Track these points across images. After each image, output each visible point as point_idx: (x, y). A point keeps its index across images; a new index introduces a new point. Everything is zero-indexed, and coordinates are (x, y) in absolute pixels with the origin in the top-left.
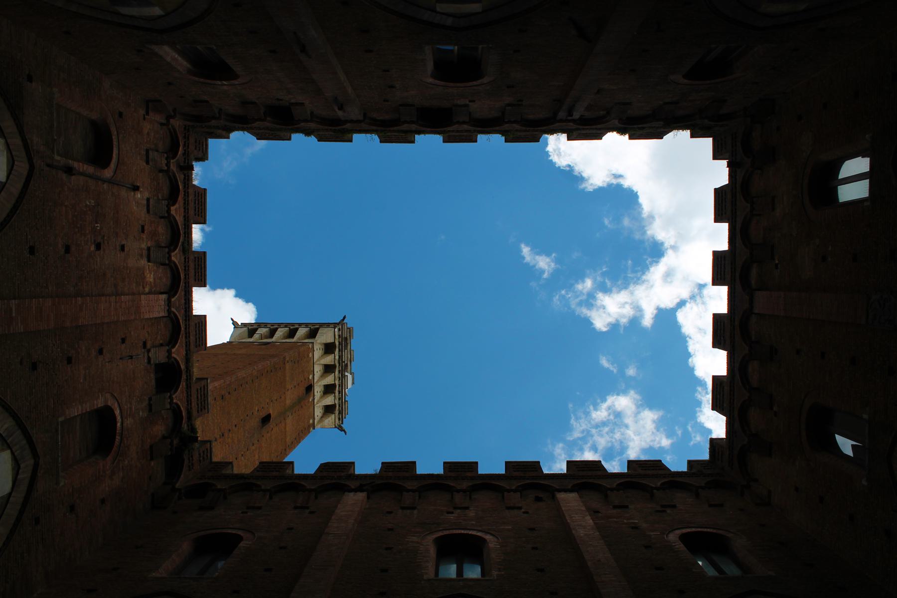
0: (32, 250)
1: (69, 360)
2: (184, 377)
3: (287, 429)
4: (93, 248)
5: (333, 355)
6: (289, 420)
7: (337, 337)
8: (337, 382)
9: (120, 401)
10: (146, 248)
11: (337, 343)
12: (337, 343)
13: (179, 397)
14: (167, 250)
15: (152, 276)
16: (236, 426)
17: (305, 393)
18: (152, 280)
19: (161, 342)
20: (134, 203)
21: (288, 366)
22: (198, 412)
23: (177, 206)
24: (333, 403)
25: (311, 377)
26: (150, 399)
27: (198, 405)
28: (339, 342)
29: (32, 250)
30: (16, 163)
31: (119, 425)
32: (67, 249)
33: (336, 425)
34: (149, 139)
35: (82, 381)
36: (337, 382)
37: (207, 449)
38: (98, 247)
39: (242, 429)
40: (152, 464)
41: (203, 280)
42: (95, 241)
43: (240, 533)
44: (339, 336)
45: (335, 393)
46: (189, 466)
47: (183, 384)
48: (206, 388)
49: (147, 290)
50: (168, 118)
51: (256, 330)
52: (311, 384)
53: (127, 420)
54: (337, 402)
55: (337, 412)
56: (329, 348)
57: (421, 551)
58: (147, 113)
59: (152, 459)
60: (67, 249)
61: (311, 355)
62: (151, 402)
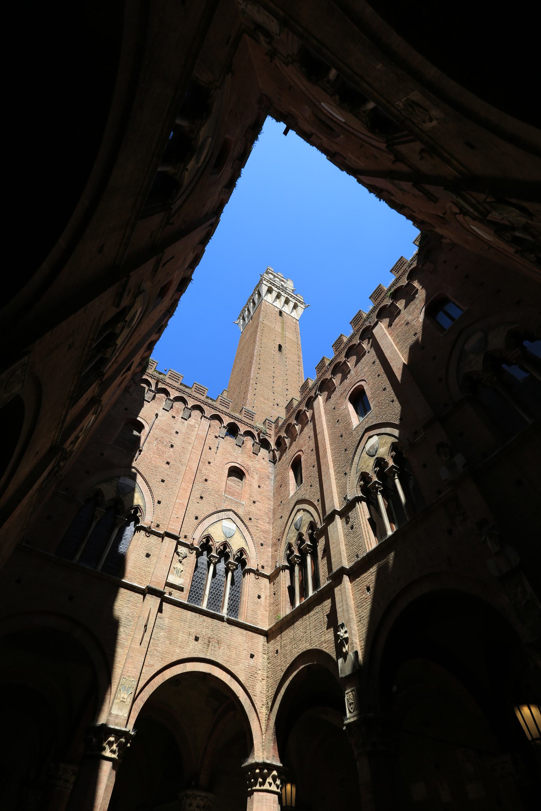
0: (163, 481)
1: (206, 480)
2: (236, 422)
3: (290, 338)
4: (172, 449)
5: (274, 291)
6: (287, 334)
7: (267, 284)
8: (286, 296)
9: (230, 461)
10: (181, 419)
11: (270, 285)
12: (270, 285)
13: (243, 429)
14: (186, 409)
15: (193, 420)
16: (274, 368)
17: (281, 317)
18: (194, 421)
19: (219, 427)
20: (162, 418)
21: (264, 322)
22: (252, 420)
23: (171, 393)
24: (294, 304)
25: (276, 309)
26: (236, 445)
27: (250, 419)
28: (270, 284)
29: (163, 481)
30: (131, 475)
31: (238, 466)
32: (168, 463)
33: (303, 308)
34: (140, 396)
35: (215, 477)
36: (286, 296)
37: (269, 423)
38: (172, 446)
39: (277, 365)
40: (259, 454)
41: (205, 390)
42: (169, 447)
43: (299, 453)
44: (267, 282)
45: (290, 300)
46: (269, 437)
47: (239, 424)
48: (246, 410)
49: (197, 426)
50: (135, 383)
51: (243, 316)
52: (280, 311)
53: (238, 460)
54: (294, 301)
55: (299, 304)
56: (270, 291)
57: (347, 413)
58: (129, 392)
59: (257, 455)
60: (168, 463)
61: (267, 304)
62: (238, 444)
